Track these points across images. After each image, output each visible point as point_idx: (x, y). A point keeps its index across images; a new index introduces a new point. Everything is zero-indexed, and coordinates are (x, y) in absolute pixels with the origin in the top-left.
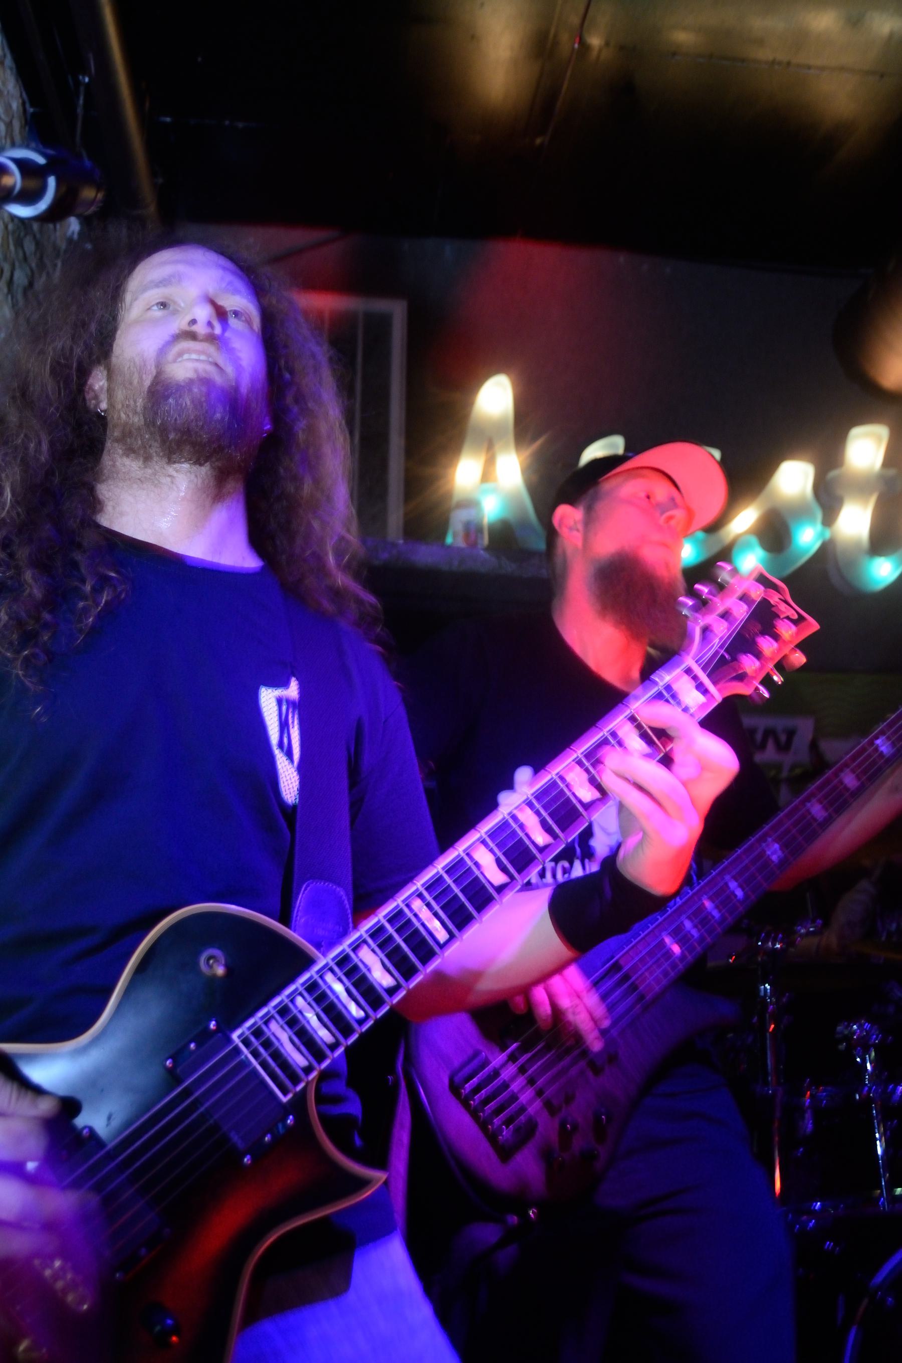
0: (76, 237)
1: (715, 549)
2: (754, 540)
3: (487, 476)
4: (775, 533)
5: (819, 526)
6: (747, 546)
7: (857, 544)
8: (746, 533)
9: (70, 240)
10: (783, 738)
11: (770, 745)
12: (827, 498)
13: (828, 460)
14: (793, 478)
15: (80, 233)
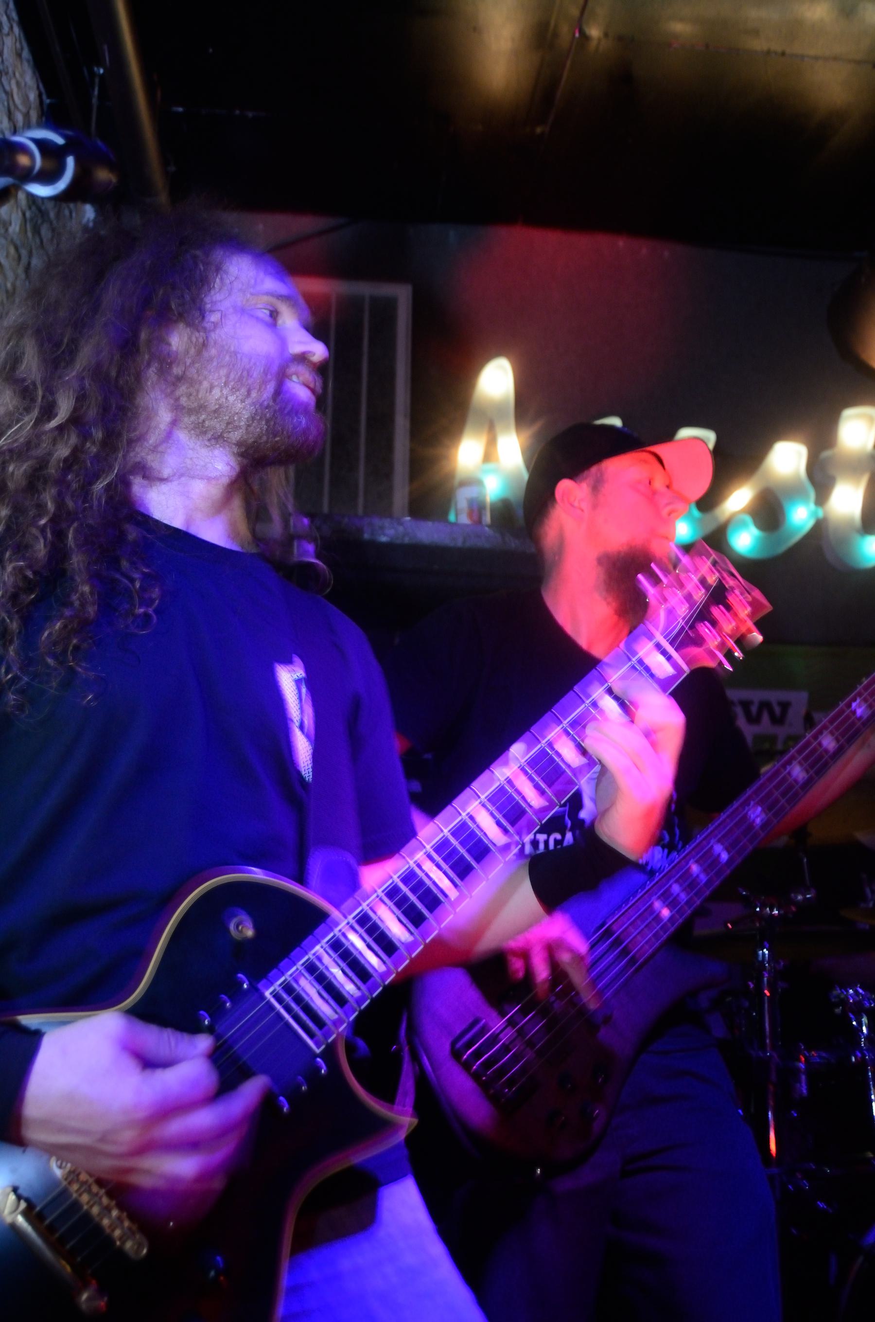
0: (91, 224)
1: (711, 527)
2: (748, 519)
3: (488, 456)
4: (769, 512)
5: (812, 506)
6: (743, 524)
7: (850, 522)
8: (743, 511)
9: (86, 229)
10: (777, 710)
11: (766, 717)
12: (820, 478)
13: (821, 440)
14: (787, 458)
15: (95, 221)
